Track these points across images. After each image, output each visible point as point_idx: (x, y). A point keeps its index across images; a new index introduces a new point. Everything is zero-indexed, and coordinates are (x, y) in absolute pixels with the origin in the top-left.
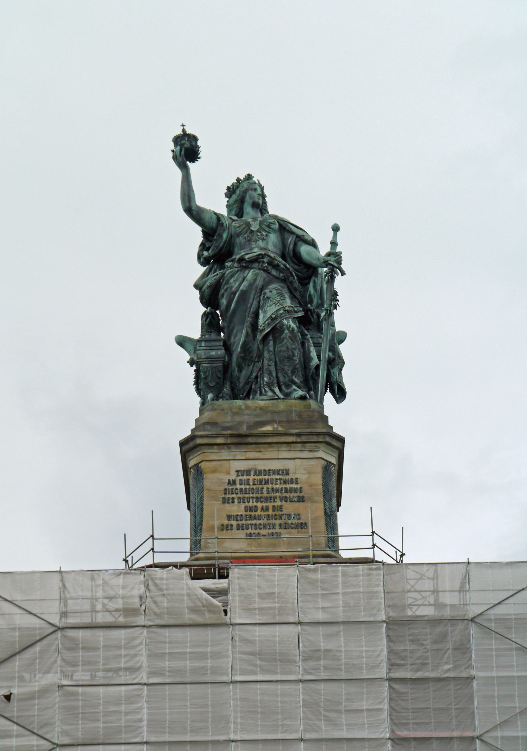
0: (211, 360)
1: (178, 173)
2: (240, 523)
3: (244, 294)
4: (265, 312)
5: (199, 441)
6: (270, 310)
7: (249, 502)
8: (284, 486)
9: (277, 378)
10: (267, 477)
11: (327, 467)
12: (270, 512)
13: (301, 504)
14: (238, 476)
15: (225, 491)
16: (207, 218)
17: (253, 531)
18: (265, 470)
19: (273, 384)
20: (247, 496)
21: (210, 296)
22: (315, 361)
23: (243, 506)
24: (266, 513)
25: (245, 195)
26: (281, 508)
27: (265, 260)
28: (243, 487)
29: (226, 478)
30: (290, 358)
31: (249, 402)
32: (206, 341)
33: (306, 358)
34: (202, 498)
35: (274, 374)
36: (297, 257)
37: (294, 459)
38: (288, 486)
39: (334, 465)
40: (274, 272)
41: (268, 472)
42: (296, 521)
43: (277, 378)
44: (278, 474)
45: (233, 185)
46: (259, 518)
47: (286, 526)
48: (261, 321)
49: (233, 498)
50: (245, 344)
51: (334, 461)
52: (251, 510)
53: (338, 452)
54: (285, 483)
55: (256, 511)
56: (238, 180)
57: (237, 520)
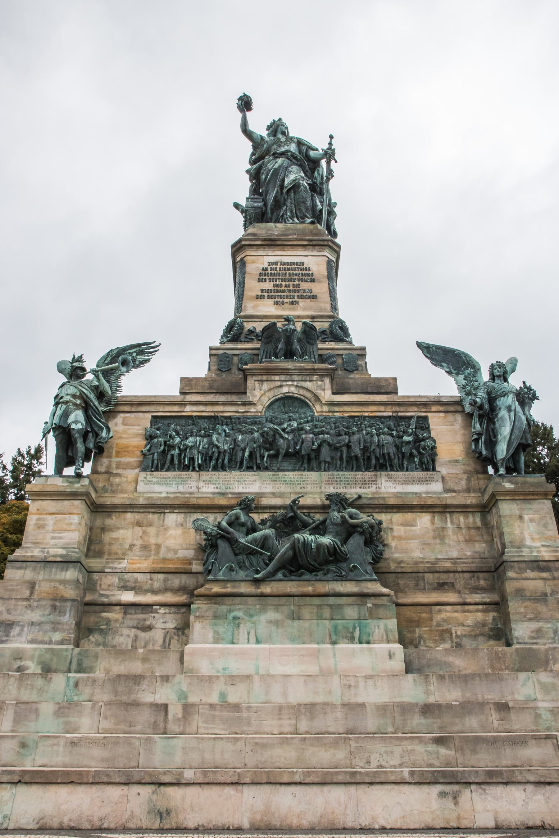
0: (254, 208)
1: (240, 115)
2: (270, 294)
3: (276, 171)
4: (289, 178)
5: (244, 243)
6: (292, 177)
7: (276, 281)
8: (301, 272)
9: (296, 214)
10: (289, 266)
11: (329, 262)
12: (291, 288)
13: (312, 283)
14: (269, 265)
15: (260, 274)
16: (255, 136)
17: (278, 300)
18: (288, 262)
19: (293, 217)
20: (275, 277)
21: (255, 176)
22: (319, 206)
23: (272, 283)
24: (288, 288)
25: (276, 128)
26: (298, 286)
27: (289, 154)
28: (273, 272)
29: (261, 267)
30: (304, 203)
31: (278, 225)
32: (251, 198)
33: (314, 205)
34: (244, 278)
35: (294, 211)
36: (307, 157)
37: (307, 256)
38: (304, 272)
39: (334, 262)
40: (294, 161)
41: (291, 264)
42: (309, 294)
43: (296, 214)
44: (297, 265)
45: (271, 124)
46: (283, 291)
47: (302, 297)
48: (287, 182)
49: (266, 279)
50: (276, 197)
51: (334, 260)
52: (278, 287)
53: (336, 255)
54: (301, 270)
55: (281, 287)
56: (274, 120)
57: (268, 293)
